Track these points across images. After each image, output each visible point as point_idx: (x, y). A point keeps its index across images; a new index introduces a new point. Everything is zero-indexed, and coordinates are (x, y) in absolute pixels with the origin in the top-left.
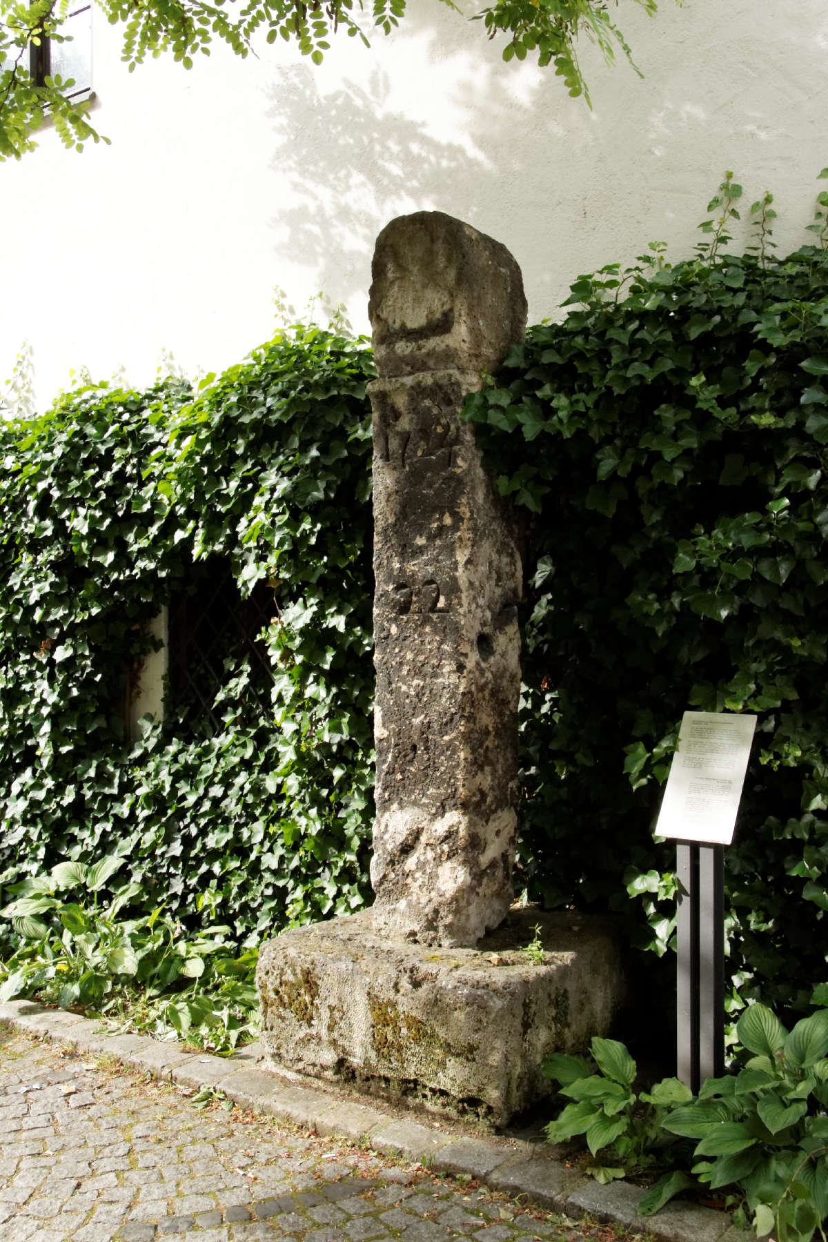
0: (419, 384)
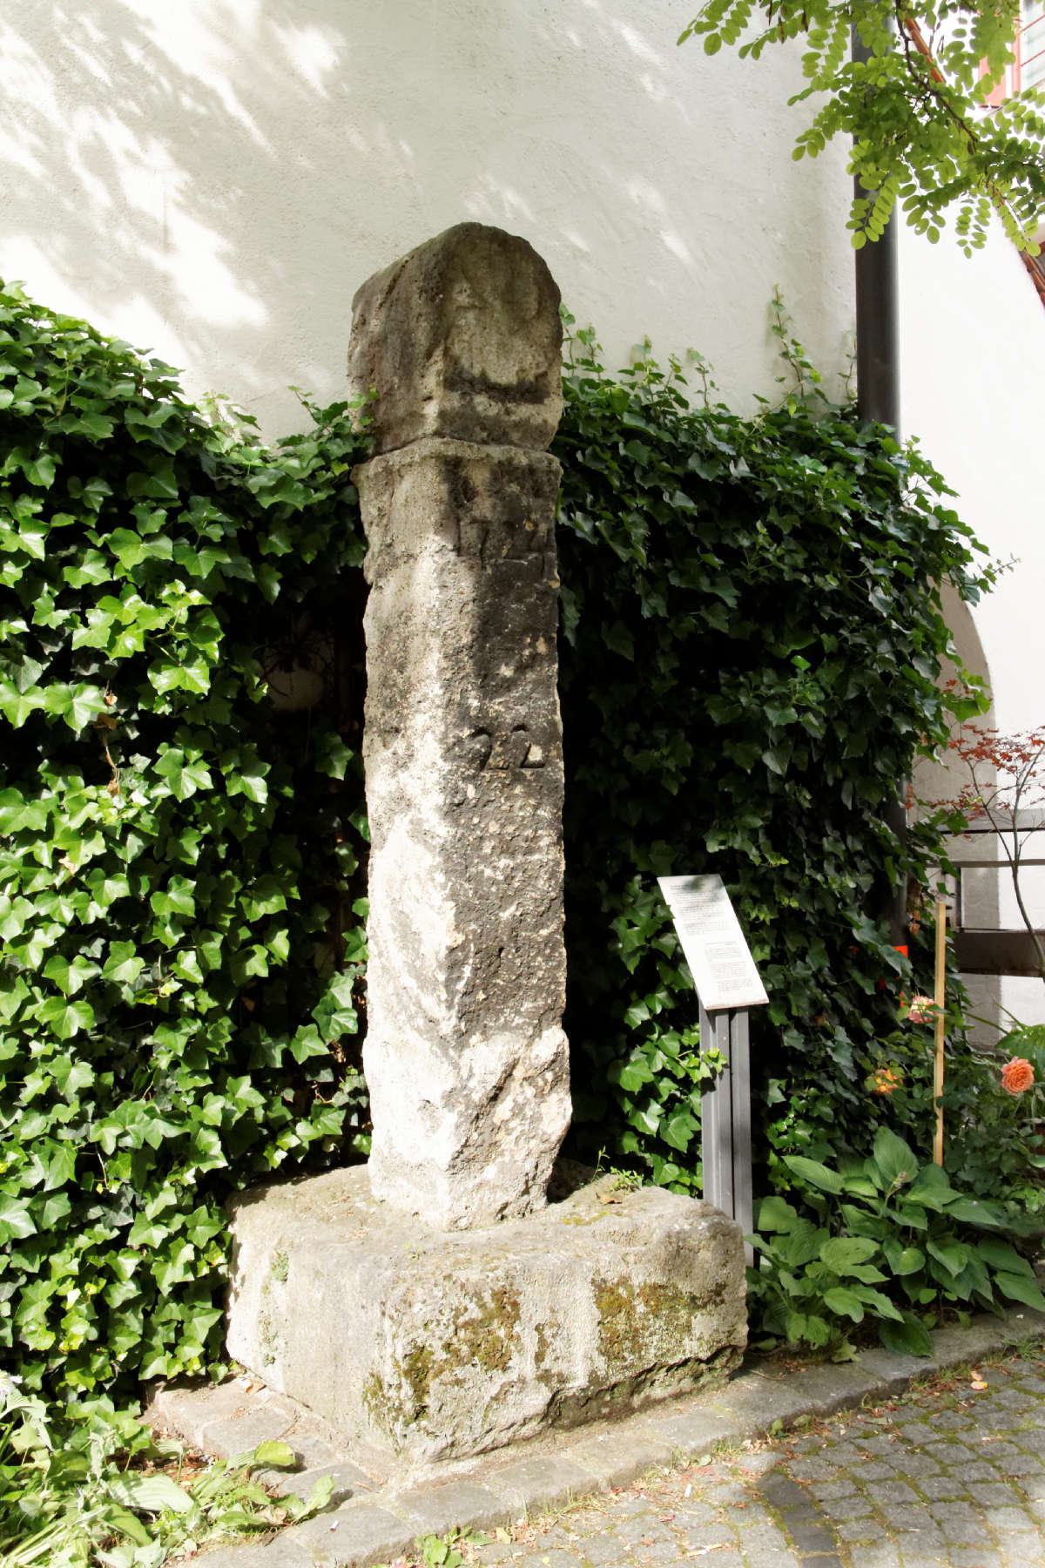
0: (510, 461)
